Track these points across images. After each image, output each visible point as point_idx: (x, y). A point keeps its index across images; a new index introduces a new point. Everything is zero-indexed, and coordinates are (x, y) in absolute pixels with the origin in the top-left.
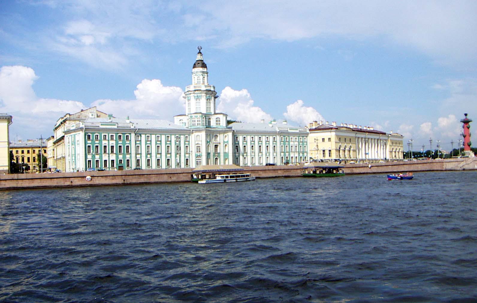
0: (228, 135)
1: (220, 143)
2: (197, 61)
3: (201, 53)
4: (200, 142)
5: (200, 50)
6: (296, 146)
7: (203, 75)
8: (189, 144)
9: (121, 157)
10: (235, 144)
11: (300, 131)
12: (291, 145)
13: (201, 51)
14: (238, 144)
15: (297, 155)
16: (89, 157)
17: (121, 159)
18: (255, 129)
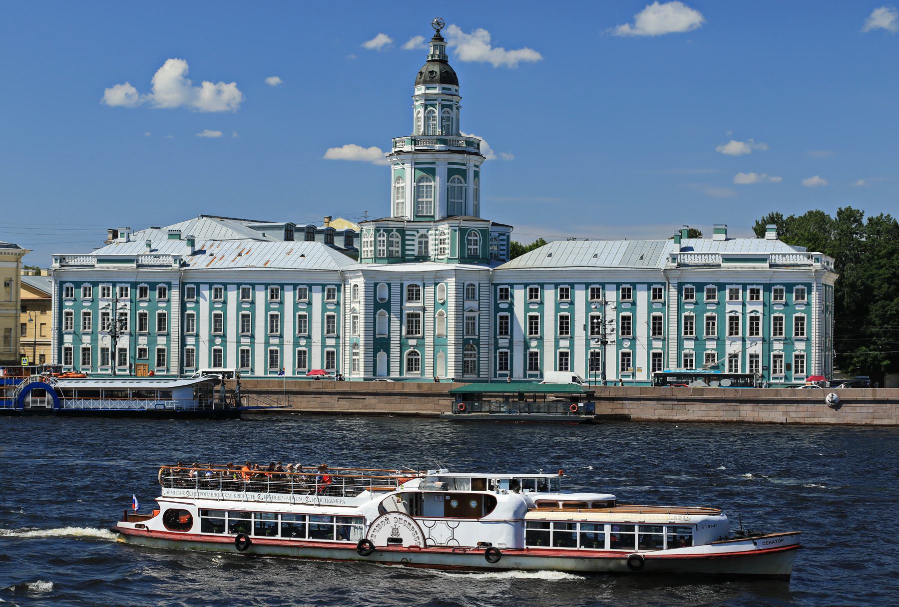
0: (446, 284)
1: (424, 309)
2: (429, 61)
3: (441, 39)
4: (356, 306)
5: (438, 31)
7: (426, 108)
8: (337, 311)
9: (143, 341)
10: (497, 309)
11: (771, 266)
12: (727, 316)
13: (442, 33)
14: (511, 309)
15: (757, 348)
16: (68, 339)
17: (145, 347)
18: (593, 262)
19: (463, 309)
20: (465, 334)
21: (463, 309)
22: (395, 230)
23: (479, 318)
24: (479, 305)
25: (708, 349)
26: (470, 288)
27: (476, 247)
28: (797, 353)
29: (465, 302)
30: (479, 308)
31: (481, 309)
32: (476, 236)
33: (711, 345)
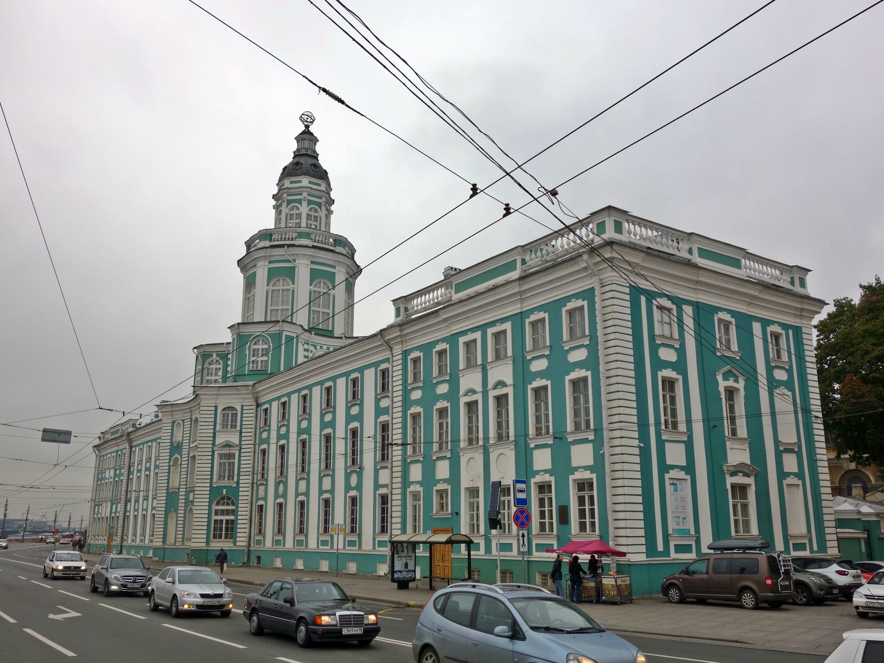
5: (307, 127)
6: (501, 400)
12: (463, 400)
19: (214, 444)
20: (214, 480)
21: (214, 444)
22: (214, 355)
23: (240, 456)
24: (241, 436)
25: (438, 481)
26: (230, 413)
27: (265, 358)
28: (578, 475)
29: (217, 434)
30: (240, 441)
31: (243, 443)
32: (266, 344)
33: (443, 470)
